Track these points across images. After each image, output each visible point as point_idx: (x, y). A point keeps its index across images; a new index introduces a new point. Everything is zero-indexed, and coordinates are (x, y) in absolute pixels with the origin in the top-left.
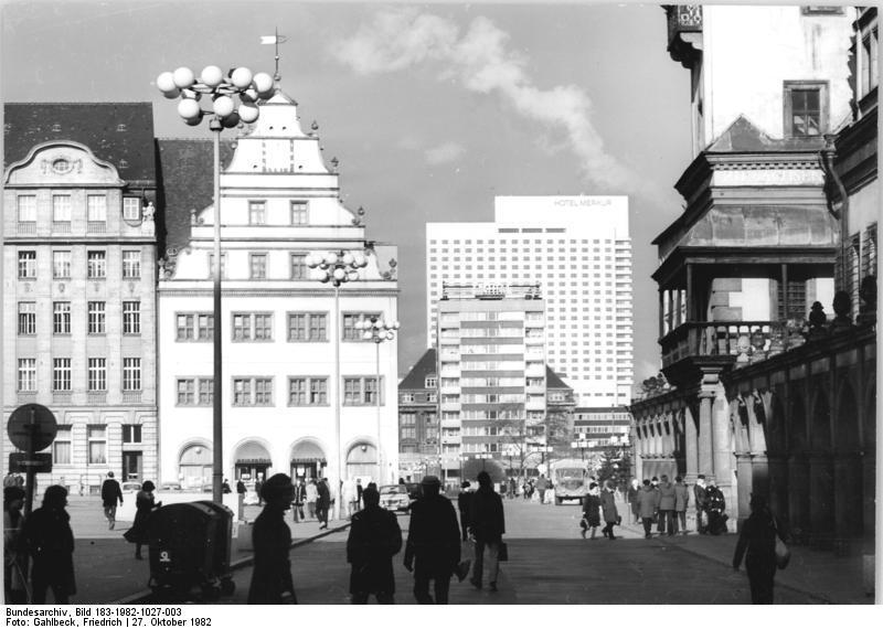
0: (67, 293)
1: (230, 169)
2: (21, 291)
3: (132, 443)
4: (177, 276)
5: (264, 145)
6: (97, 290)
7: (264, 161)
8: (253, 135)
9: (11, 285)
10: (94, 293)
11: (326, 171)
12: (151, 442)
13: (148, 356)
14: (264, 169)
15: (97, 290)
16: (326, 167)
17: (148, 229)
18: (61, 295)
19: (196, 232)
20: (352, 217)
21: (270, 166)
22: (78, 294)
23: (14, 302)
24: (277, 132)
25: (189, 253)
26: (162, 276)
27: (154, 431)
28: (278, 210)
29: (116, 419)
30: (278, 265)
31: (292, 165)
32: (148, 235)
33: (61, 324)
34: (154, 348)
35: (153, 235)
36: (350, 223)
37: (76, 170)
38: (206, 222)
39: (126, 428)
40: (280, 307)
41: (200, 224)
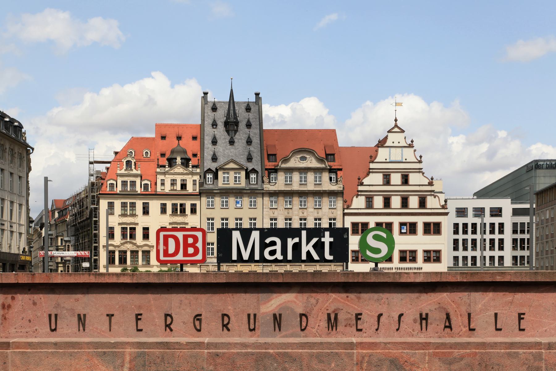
2: (286, 213)
8: (386, 145)
18: (303, 215)
21: (393, 159)
23: (283, 218)
24: (396, 144)
28: (396, 179)
30: (396, 202)
31: (402, 158)
37: (309, 162)
40: (396, 221)
41: (362, 184)
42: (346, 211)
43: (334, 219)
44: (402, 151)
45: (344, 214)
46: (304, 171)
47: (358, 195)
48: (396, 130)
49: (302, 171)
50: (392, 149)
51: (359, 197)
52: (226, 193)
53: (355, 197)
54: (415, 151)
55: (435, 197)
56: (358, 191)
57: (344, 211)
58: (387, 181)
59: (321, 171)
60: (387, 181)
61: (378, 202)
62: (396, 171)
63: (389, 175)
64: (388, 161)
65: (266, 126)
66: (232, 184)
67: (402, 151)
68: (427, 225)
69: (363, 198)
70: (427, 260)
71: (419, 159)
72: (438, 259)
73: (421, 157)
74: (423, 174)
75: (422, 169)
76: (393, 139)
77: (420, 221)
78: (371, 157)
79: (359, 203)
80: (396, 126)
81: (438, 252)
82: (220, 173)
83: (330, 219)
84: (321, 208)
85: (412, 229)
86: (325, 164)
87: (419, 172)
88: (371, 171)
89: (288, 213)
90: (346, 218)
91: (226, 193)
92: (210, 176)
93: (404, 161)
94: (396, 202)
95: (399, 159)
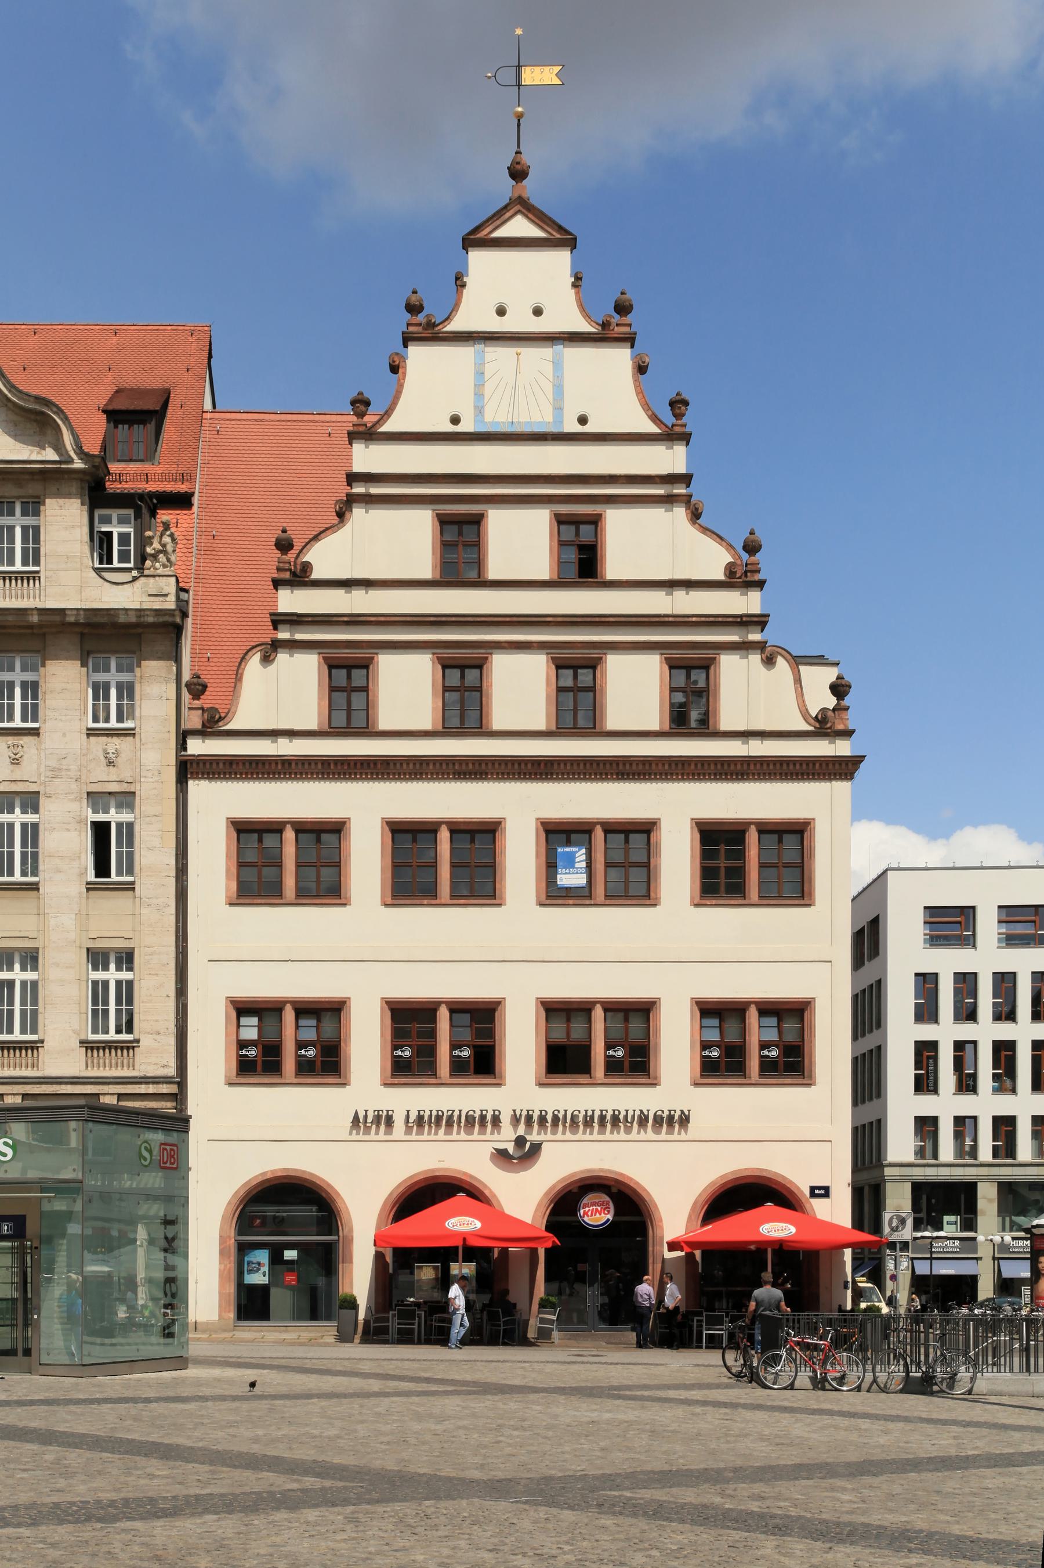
6: (16, 761)
15: (16, 761)
21: (497, 418)
24: (519, 321)
30: (520, 690)
36: (720, 576)
40: (520, 810)
42: (196, 747)
43: (126, 799)
47: (276, 645)
50: (499, 355)
51: (282, 657)
53: (255, 659)
56: (279, 620)
59: (33, 488)
61: (406, 690)
62: (520, 491)
63: (477, 521)
69: (309, 664)
70: (722, 1064)
78: (361, 404)
79: (280, 695)
81: (792, 1014)
83: (96, 799)
84: (35, 732)
85: (623, 861)
86: (59, 447)
90: (196, 788)
94: (520, 690)
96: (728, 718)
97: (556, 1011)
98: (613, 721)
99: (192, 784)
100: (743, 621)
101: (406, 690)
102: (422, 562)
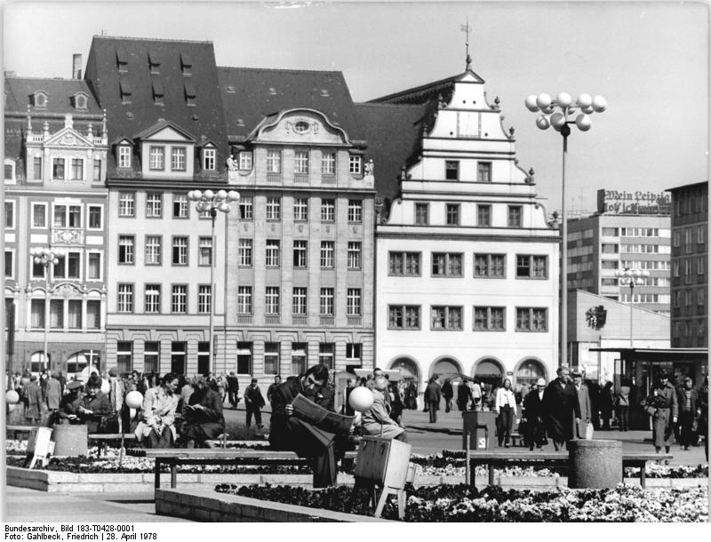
0: (305, 232)
1: (432, 135)
3: (353, 358)
4: (391, 222)
5: (458, 115)
7: (458, 128)
9: (261, 224)
10: (326, 234)
11: (506, 139)
12: (368, 358)
13: (368, 288)
14: (458, 135)
15: (328, 231)
16: (506, 135)
17: (368, 182)
18: (300, 235)
19: (406, 186)
20: (525, 177)
21: (463, 133)
22: (315, 232)
24: (469, 105)
25: (399, 203)
26: (379, 221)
27: (372, 348)
29: (342, 339)
30: (469, 214)
31: (480, 132)
32: (368, 187)
33: (299, 258)
34: (372, 280)
35: (372, 187)
36: (523, 182)
38: (413, 178)
39: (349, 346)
40: (469, 249)
41: (408, 179)
42: (380, 229)
44: (480, 117)
45: (376, 235)
46: (303, 149)
48: (469, 78)
49: (300, 150)
52: (155, 189)
54: (502, 119)
55: (537, 208)
57: (375, 228)
58: (452, 174)
60: (452, 174)
61: (437, 213)
62: (469, 154)
63: (457, 163)
64: (454, 136)
65: (217, 65)
66: (168, 174)
67: (480, 117)
68: (523, 260)
71: (509, 135)
72: (543, 326)
73: (512, 131)
74: (516, 163)
75: (514, 153)
76: (461, 93)
77: (511, 251)
80: (468, 70)
81: (542, 311)
82: (146, 147)
87: (510, 159)
88: (425, 153)
89: (273, 230)
90: (380, 242)
91: (155, 189)
92: (125, 152)
93: (483, 137)
94: (469, 214)
95: (473, 133)
96: (526, 224)
97: (478, 309)
98: (494, 224)
99: (378, 240)
100: (531, 196)
101: (437, 213)
102: (442, 175)
